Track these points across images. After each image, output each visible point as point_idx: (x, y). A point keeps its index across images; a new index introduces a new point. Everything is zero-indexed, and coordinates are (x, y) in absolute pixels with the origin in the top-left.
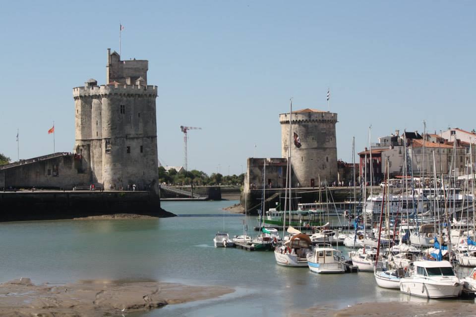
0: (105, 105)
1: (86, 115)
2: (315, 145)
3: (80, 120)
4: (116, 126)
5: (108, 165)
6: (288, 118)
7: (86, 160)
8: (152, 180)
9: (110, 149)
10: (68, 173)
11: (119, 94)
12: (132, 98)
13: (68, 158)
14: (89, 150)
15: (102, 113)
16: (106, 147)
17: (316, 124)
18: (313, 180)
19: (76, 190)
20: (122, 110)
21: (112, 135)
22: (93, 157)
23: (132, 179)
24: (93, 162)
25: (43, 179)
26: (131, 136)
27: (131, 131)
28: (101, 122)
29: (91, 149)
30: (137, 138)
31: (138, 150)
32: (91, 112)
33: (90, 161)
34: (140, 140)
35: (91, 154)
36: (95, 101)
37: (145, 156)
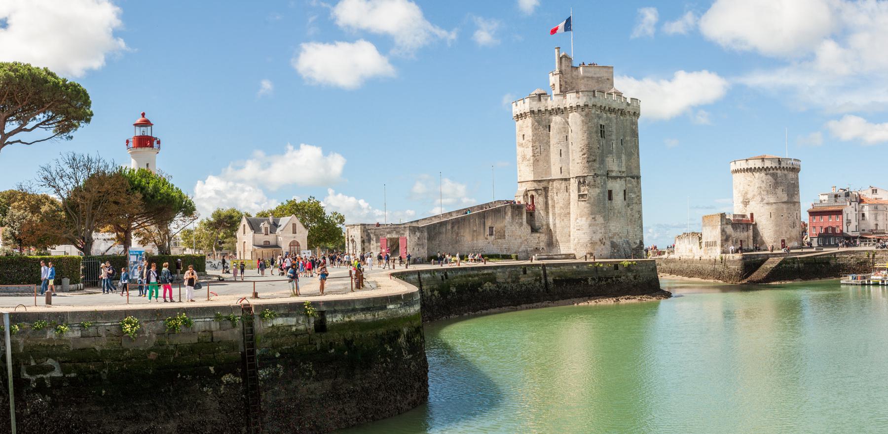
0: (576, 123)
1: (540, 142)
2: (785, 199)
3: (531, 149)
4: (595, 156)
5: (584, 219)
6: (752, 164)
7: (541, 212)
8: (638, 242)
9: (586, 192)
10: (517, 235)
11: (599, 105)
12: (613, 115)
13: (517, 208)
14: (546, 197)
15: (569, 137)
16: (579, 190)
17: (786, 172)
18: (783, 241)
19: (539, 259)
20: (602, 131)
21: (590, 168)
22: (553, 206)
23: (615, 240)
24: (554, 214)
25: (485, 243)
26: (614, 174)
27: (613, 165)
28: (568, 152)
29: (550, 194)
30: (620, 178)
31: (622, 194)
32: (549, 137)
33: (548, 213)
34: (623, 181)
35: (550, 202)
36: (556, 119)
37: (628, 205)
